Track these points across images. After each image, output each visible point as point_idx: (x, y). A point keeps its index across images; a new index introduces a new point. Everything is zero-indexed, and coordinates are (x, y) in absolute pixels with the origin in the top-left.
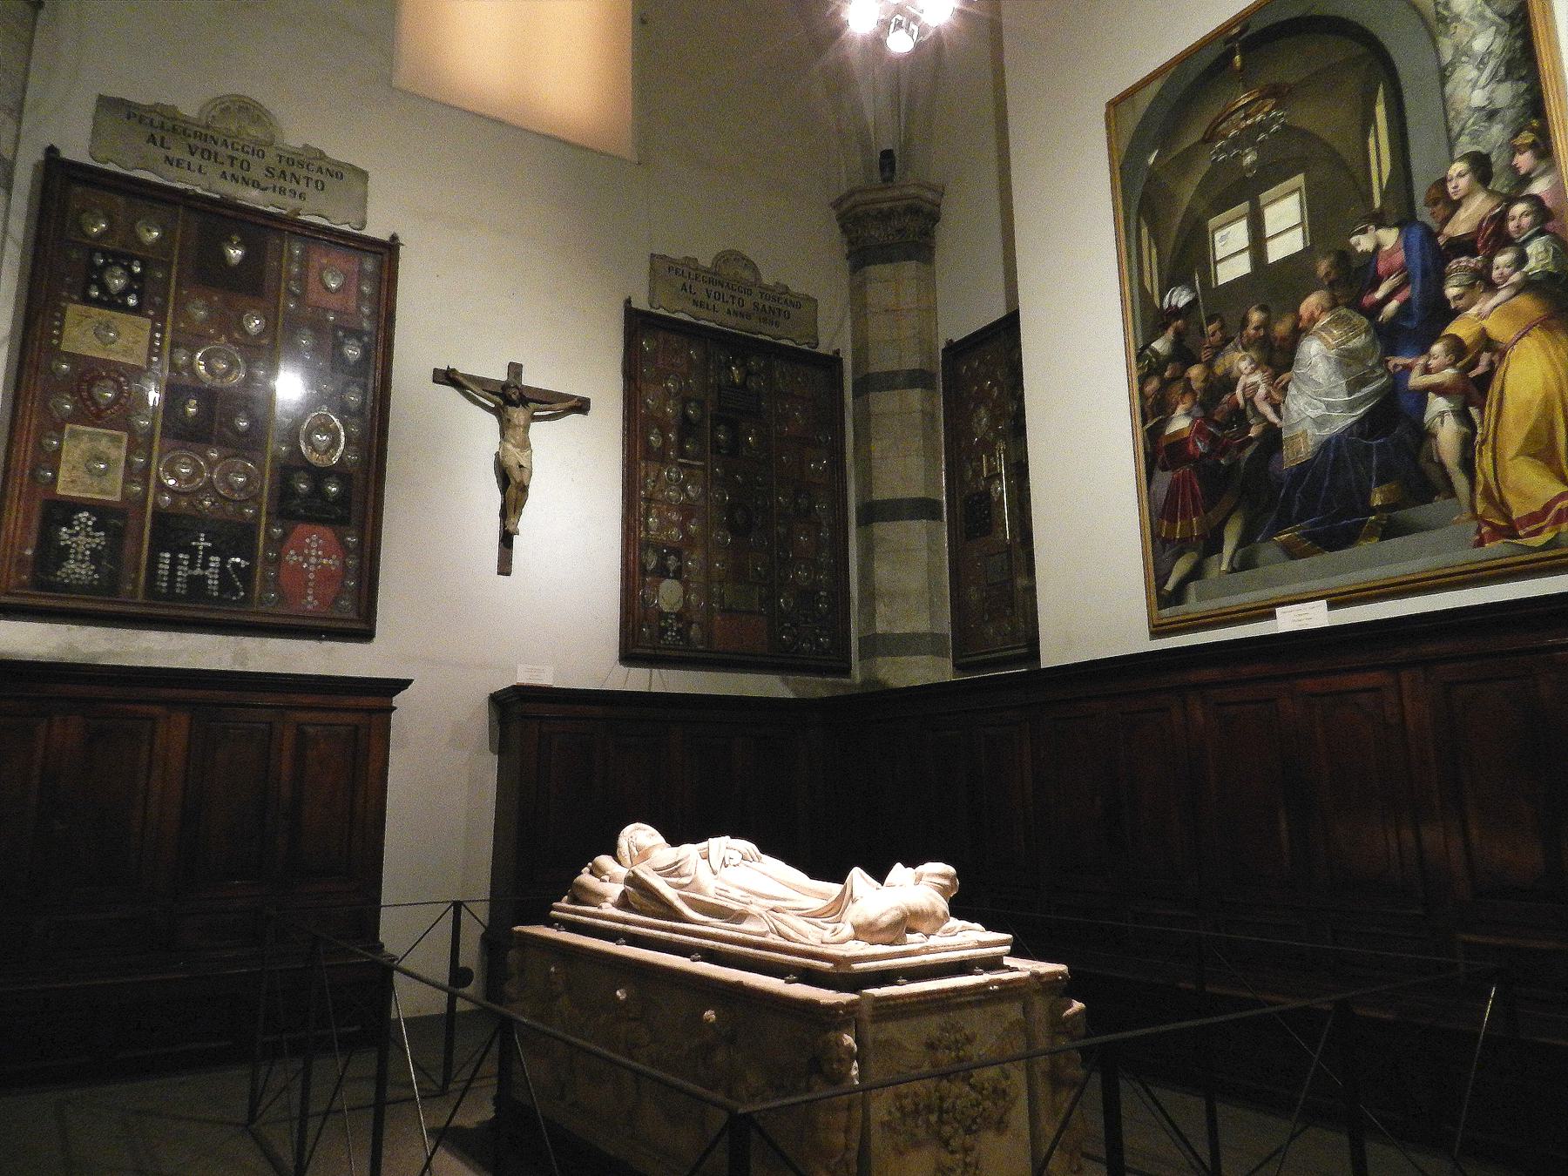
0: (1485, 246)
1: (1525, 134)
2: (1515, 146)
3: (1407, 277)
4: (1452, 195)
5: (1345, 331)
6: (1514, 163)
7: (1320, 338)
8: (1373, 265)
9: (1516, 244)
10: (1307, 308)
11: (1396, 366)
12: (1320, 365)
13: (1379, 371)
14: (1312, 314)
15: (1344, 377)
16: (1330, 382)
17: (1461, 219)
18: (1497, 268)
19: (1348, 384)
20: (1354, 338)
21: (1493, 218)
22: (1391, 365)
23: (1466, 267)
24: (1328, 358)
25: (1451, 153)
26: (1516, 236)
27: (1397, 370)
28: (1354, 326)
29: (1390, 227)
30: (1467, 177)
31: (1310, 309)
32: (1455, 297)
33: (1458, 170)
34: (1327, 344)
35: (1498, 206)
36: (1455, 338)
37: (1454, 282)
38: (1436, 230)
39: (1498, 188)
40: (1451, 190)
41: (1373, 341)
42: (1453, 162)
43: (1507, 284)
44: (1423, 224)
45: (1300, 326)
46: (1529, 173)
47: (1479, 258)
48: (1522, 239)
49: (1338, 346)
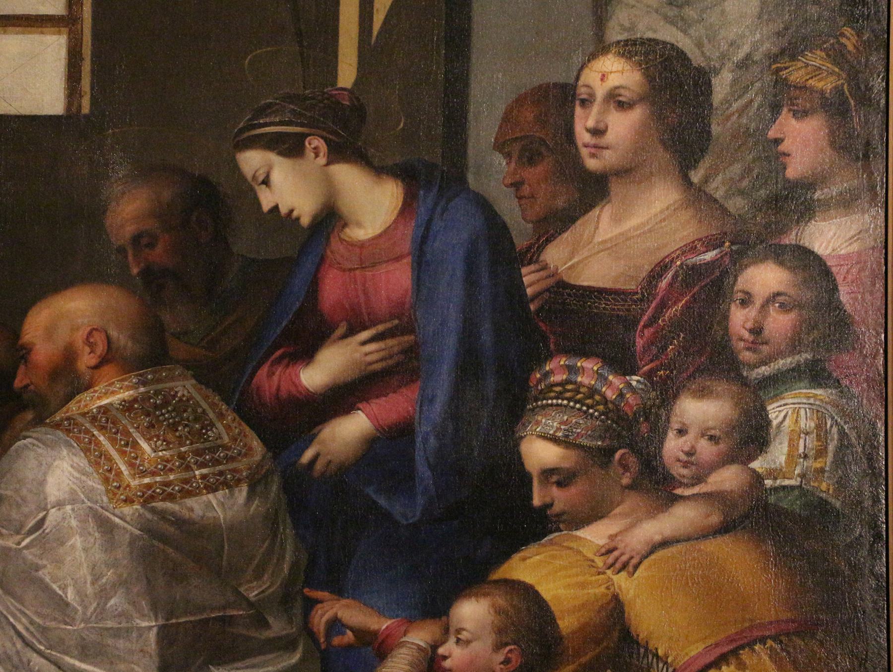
0: (660, 341)
1: (816, 59)
2: (781, 84)
3: (411, 352)
4: (584, 152)
5: (182, 456)
6: (772, 134)
7: (98, 459)
8: (308, 265)
9: (744, 382)
10: (50, 332)
11: (335, 625)
12: (77, 541)
13: (278, 627)
14: (69, 356)
15: (155, 607)
16: (101, 613)
17: (599, 238)
18: (682, 432)
19: (166, 636)
20: (212, 489)
21: (694, 272)
22: (321, 618)
23: (592, 392)
24: (106, 527)
25: (600, 22)
26: (747, 356)
27: (336, 641)
28: (213, 450)
29: (379, 170)
30: (637, 114)
31: (62, 336)
32: (548, 473)
33: (614, 81)
34: (110, 476)
35: (711, 243)
36: (528, 593)
37: (551, 423)
38: (520, 242)
39: (717, 188)
40: (583, 137)
41: (272, 521)
42: (601, 48)
43: (696, 490)
44: (484, 206)
45: (18, 383)
46: (809, 184)
47: (634, 380)
48: (764, 370)
49: (147, 497)
